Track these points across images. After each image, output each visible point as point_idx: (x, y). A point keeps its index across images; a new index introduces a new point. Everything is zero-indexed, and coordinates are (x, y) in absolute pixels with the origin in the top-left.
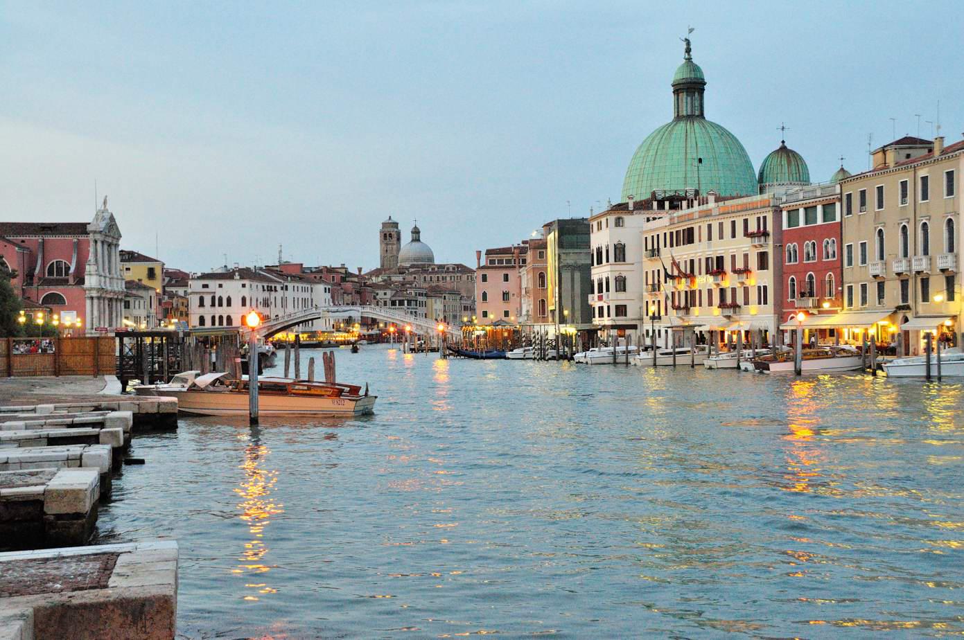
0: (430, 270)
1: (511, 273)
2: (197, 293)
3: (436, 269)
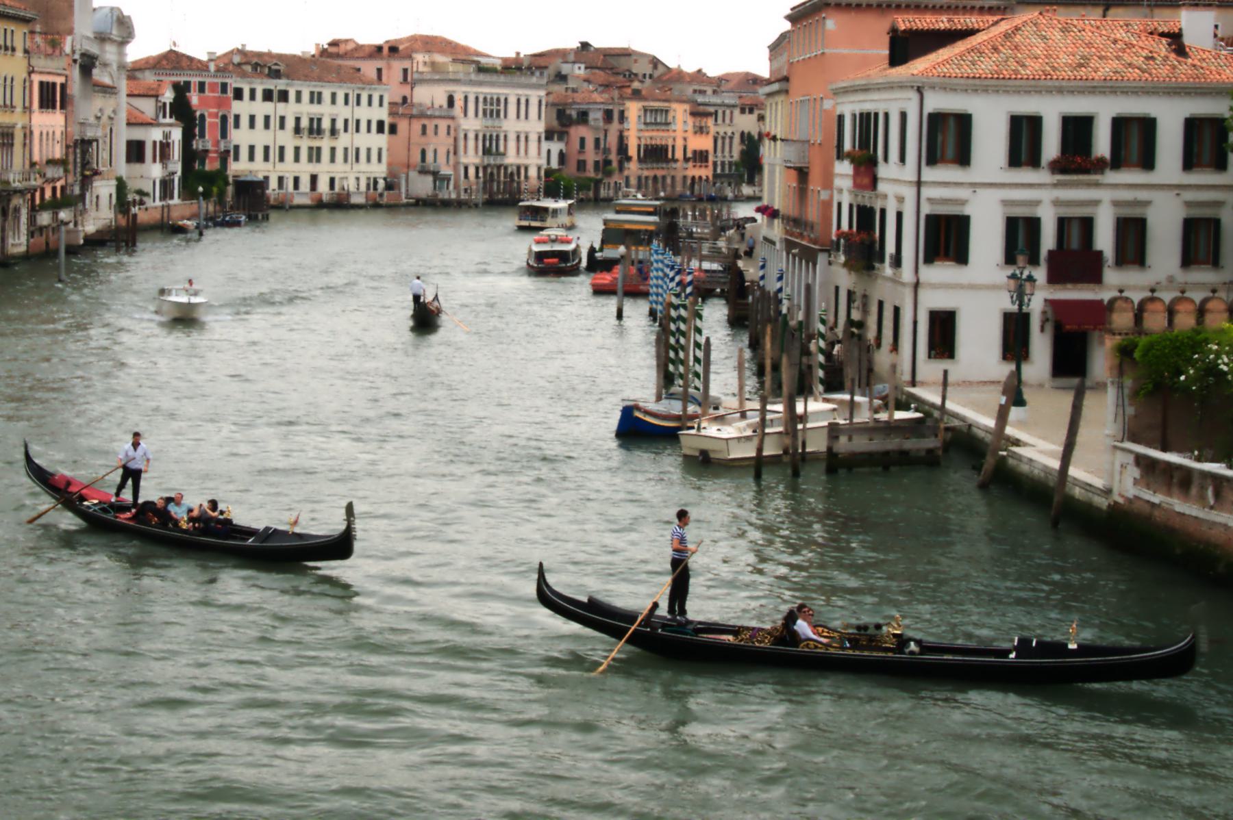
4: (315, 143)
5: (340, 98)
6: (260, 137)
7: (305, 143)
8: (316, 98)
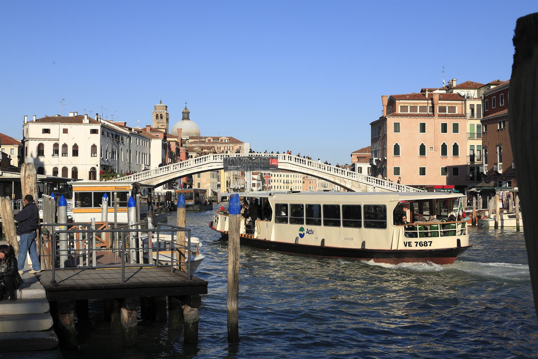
0: (207, 141)
1: (427, 121)
2: (35, 139)
3: (212, 141)
4: (288, 185)
5: (292, 176)
6: (276, 184)
7: (286, 185)
8: (287, 176)
